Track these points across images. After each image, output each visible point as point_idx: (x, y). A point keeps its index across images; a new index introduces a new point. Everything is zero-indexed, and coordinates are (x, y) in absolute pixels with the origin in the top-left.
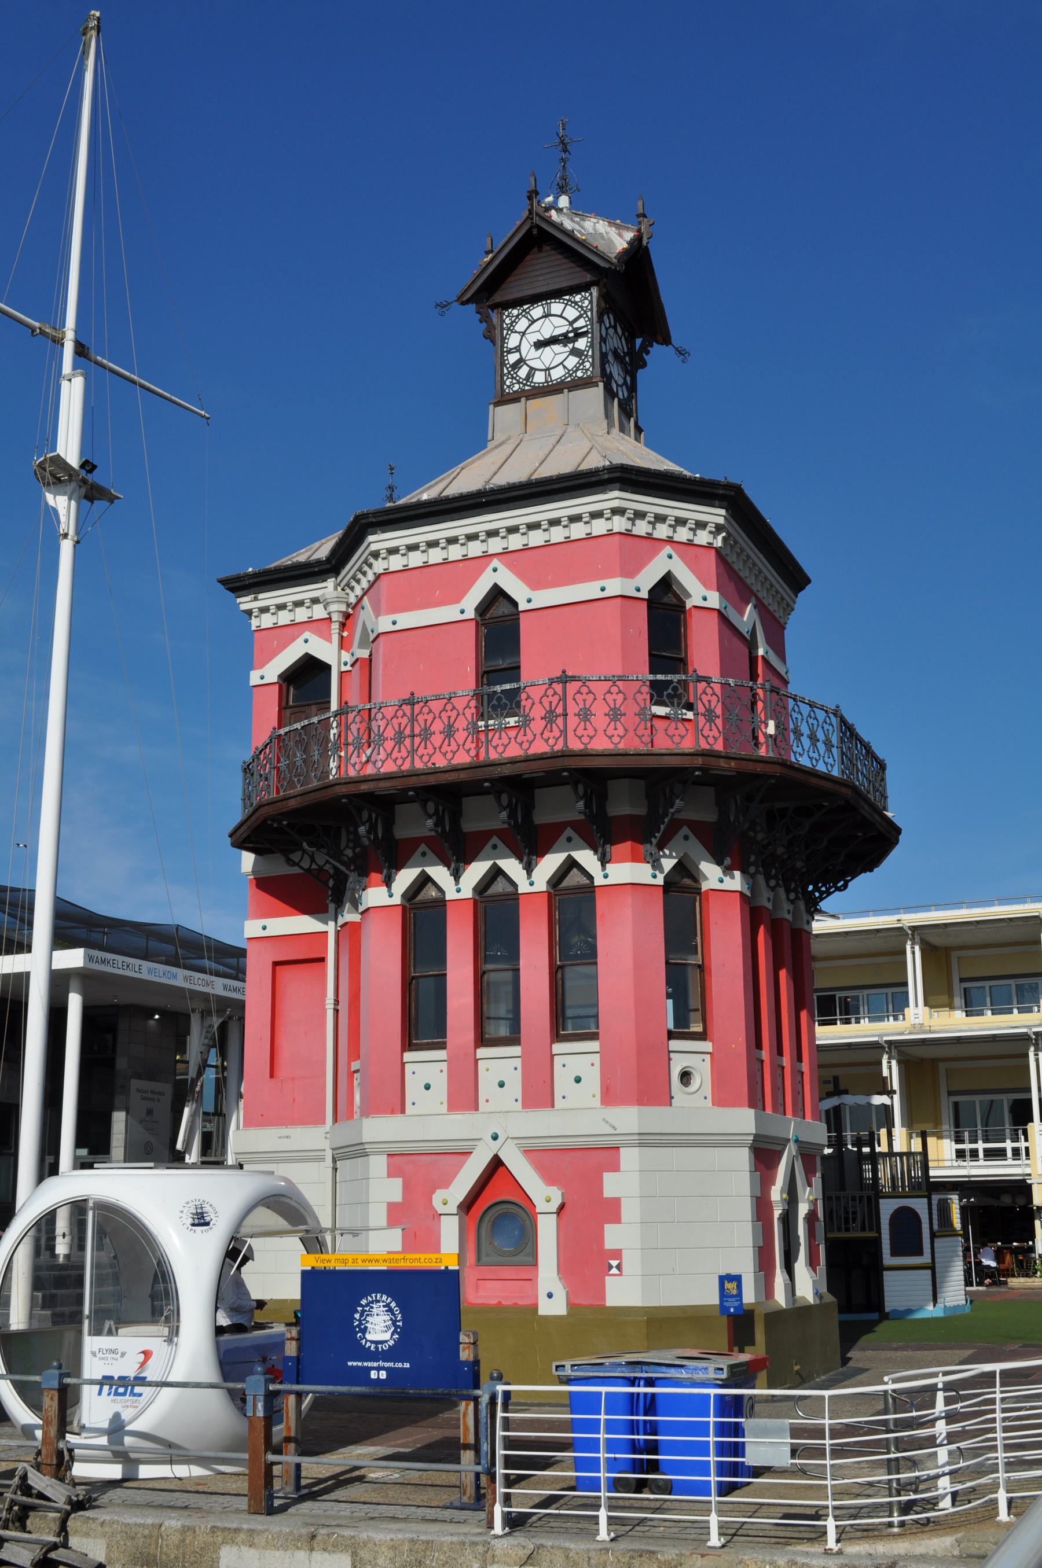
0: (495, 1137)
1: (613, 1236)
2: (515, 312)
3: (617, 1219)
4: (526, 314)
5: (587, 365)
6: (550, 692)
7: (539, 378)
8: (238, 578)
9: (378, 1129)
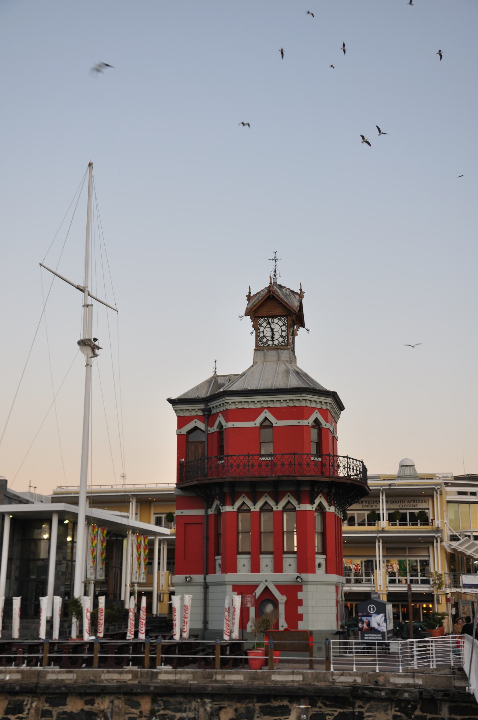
0: (266, 581)
1: (300, 610)
2: (262, 320)
3: (301, 605)
5: (286, 341)
6: (290, 457)
7: (270, 343)
8: (174, 400)
9: (230, 577)
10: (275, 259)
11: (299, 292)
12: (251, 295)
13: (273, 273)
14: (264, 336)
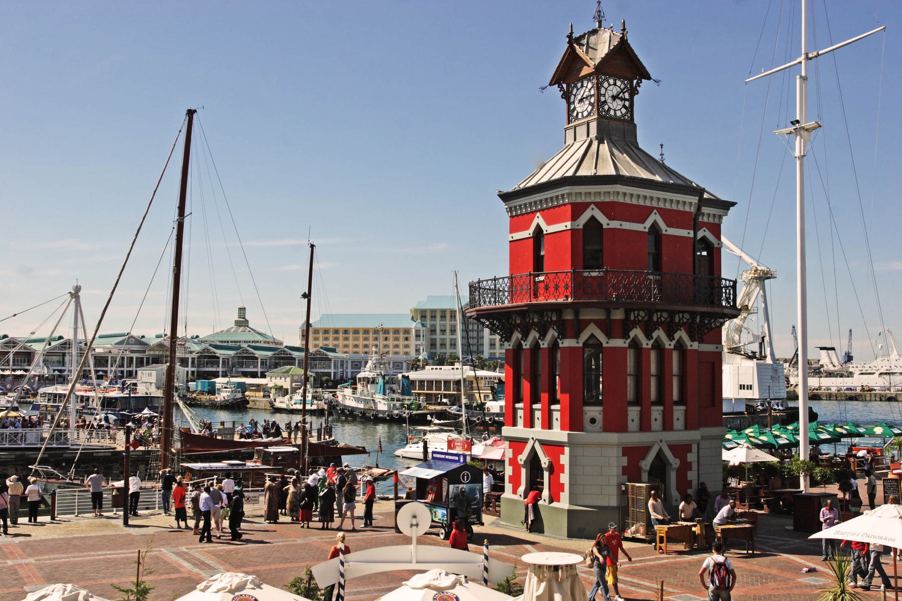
14: (605, 102)
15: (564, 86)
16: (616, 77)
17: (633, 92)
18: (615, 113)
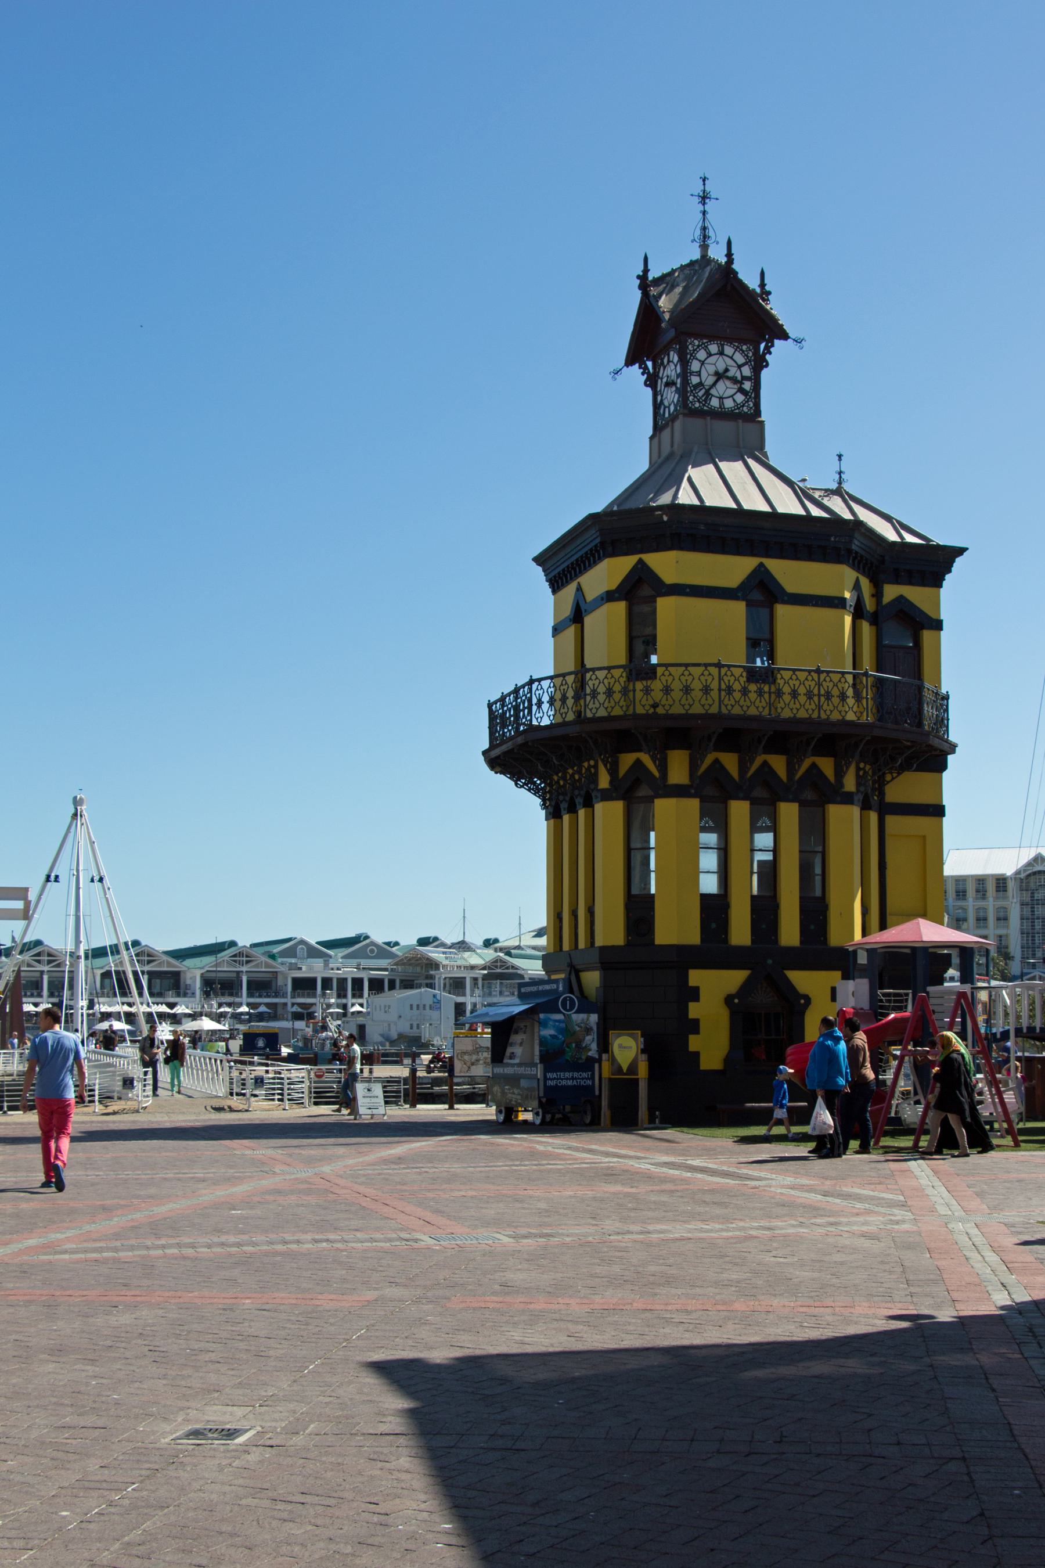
2: (696, 342)
4: (706, 348)
7: (715, 403)
10: (704, 198)
11: (758, 290)
12: (650, 278)
13: (698, 232)
15: (650, 364)
16: (723, 338)
17: (759, 363)
18: (722, 404)
